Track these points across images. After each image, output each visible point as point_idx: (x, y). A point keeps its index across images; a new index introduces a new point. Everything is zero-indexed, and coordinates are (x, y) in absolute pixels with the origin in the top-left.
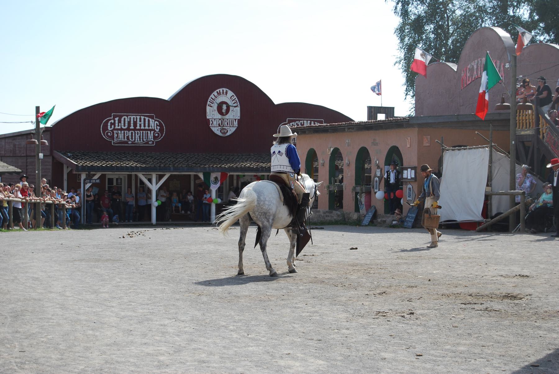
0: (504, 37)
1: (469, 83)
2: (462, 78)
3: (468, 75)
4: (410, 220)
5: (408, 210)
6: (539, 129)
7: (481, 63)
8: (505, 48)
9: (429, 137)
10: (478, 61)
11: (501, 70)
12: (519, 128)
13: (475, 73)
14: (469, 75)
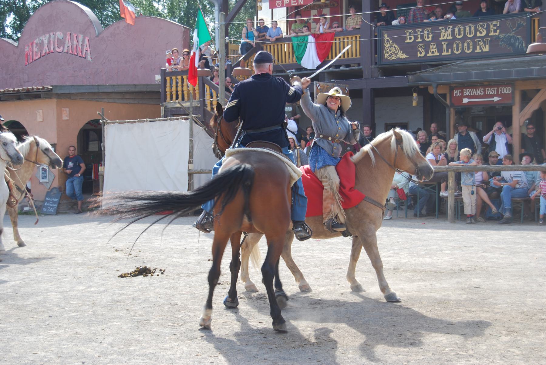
0: (88, 11)
1: (37, 58)
2: (26, 53)
3: (35, 49)
4: (51, 205)
5: (45, 194)
6: (204, 101)
7: (55, 37)
8: (91, 22)
9: (68, 109)
10: (50, 36)
11: (85, 44)
12: (171, 99)
13: (46, 47)
14: (37, 50)
